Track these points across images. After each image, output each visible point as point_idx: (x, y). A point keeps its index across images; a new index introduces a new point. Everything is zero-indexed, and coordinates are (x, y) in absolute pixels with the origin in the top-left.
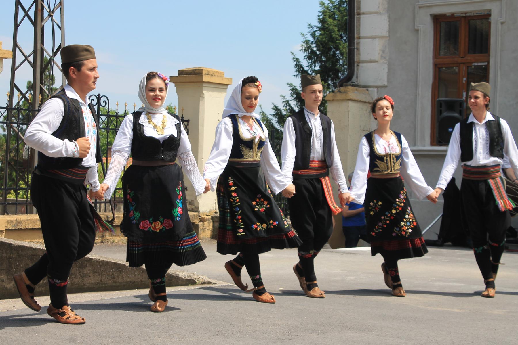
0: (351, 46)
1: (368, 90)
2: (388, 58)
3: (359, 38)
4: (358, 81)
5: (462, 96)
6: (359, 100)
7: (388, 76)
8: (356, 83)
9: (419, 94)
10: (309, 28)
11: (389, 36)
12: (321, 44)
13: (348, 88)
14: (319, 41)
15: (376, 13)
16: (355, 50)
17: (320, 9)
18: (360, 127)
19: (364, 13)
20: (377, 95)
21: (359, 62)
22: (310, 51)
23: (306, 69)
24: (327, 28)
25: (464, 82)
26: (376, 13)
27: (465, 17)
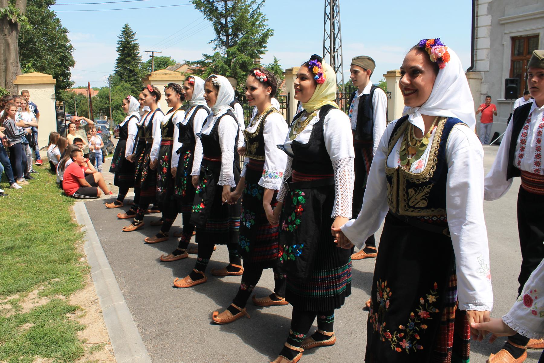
3: (477, 49)
7: (490, 67)
15: (484, 37)
16: (475, 55)
19: (479, 38)
21: (476, 60)
26: (484, 37)
27: (527, 37)
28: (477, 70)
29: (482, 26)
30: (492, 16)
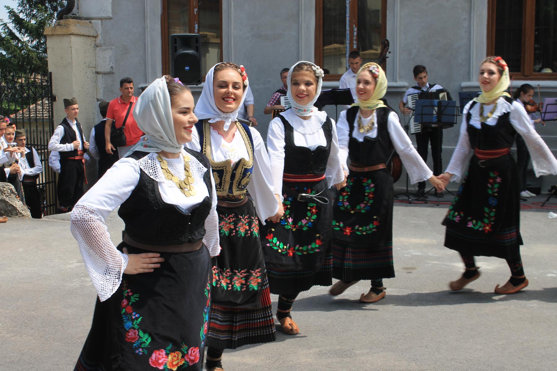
1: (91, 22)
4: (80, 12)
5: (194, 28)
6: (82, 34)
7: (113, 6)
8: (78, 15)
9: (147, 26)
13: (68, 21)
18: (85, 63)
20: (102, 27)
25: (195, 13)
28: (84, 15)
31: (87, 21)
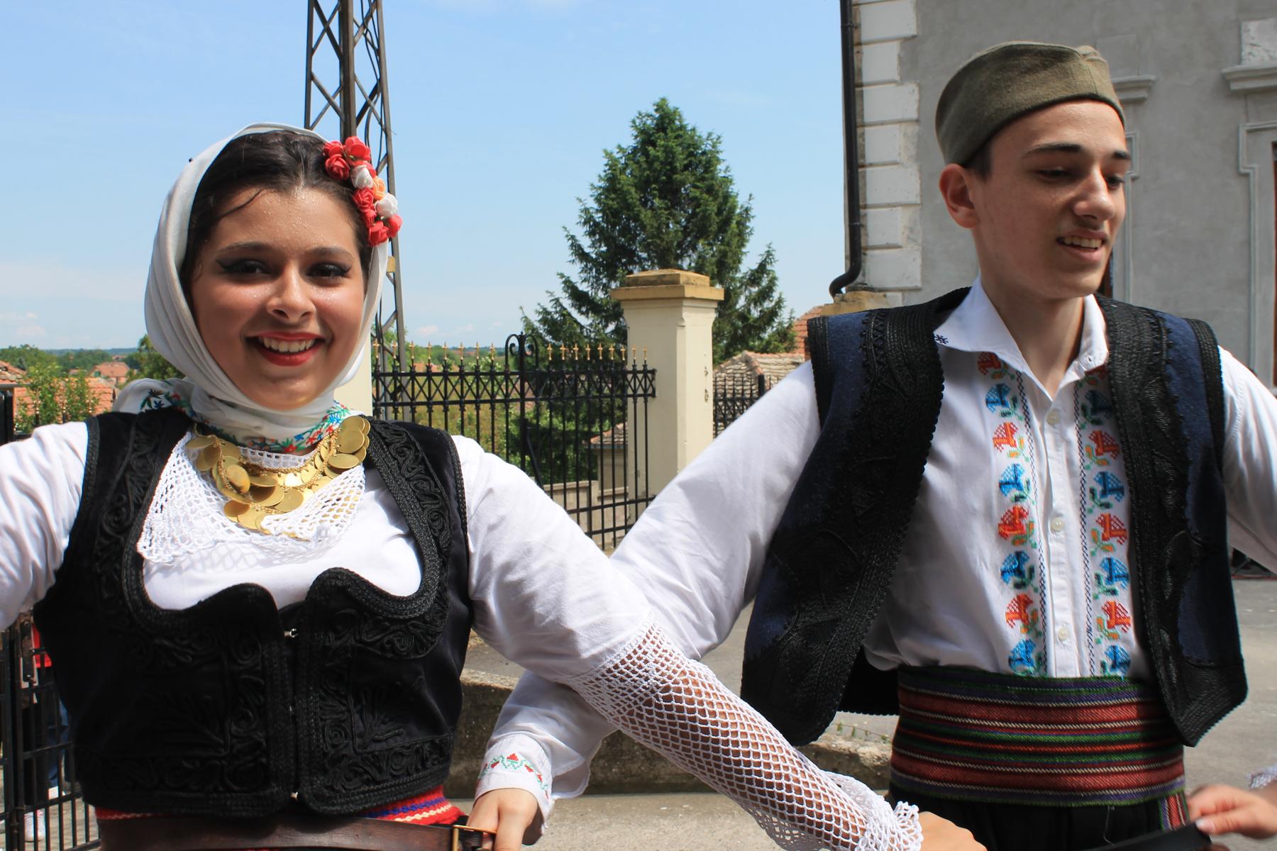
0: (855, 221)
1: (885, 296)
2: (920, 241)
8: (869, 285)
10: (591, 189)
11: (922, 204)
12: (611, 213)
14: (609, 208)
17: (606, 161)
19: (871, 165)
22: (592, 223)
23: (587, 250)
24: (619, 189)
29: (882, 123)
30: (920, 87)
31: (881, 294)
